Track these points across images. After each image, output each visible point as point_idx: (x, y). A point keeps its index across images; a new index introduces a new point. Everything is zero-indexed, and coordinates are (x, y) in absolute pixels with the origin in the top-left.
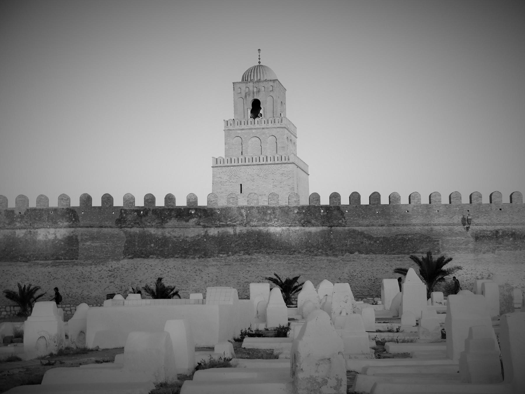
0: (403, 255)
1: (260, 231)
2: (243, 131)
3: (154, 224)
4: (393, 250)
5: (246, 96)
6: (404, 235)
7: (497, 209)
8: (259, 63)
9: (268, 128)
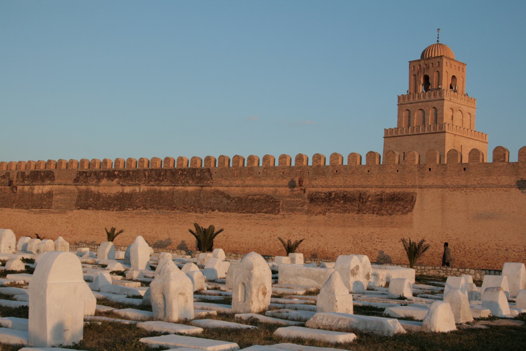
0: (251, 214)
1: (156, 189)
2: (412, 105)
3: (94, 183)
4: (244, 209)
5: (418, 74)
6: (254, 195)
7: (333, 171)
8: (438, 41)
9: (430, 101)
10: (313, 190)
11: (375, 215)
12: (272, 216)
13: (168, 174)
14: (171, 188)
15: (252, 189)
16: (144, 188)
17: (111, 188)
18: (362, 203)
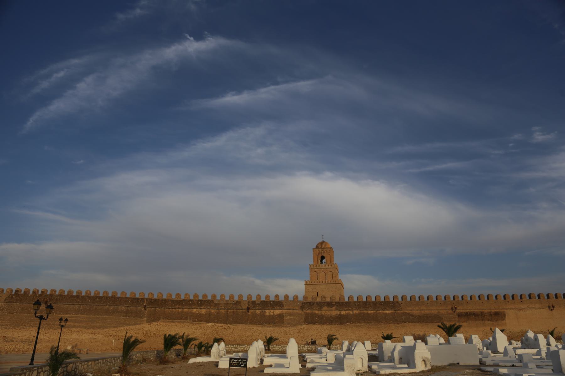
13: (371, 304)
15: (426, 311)
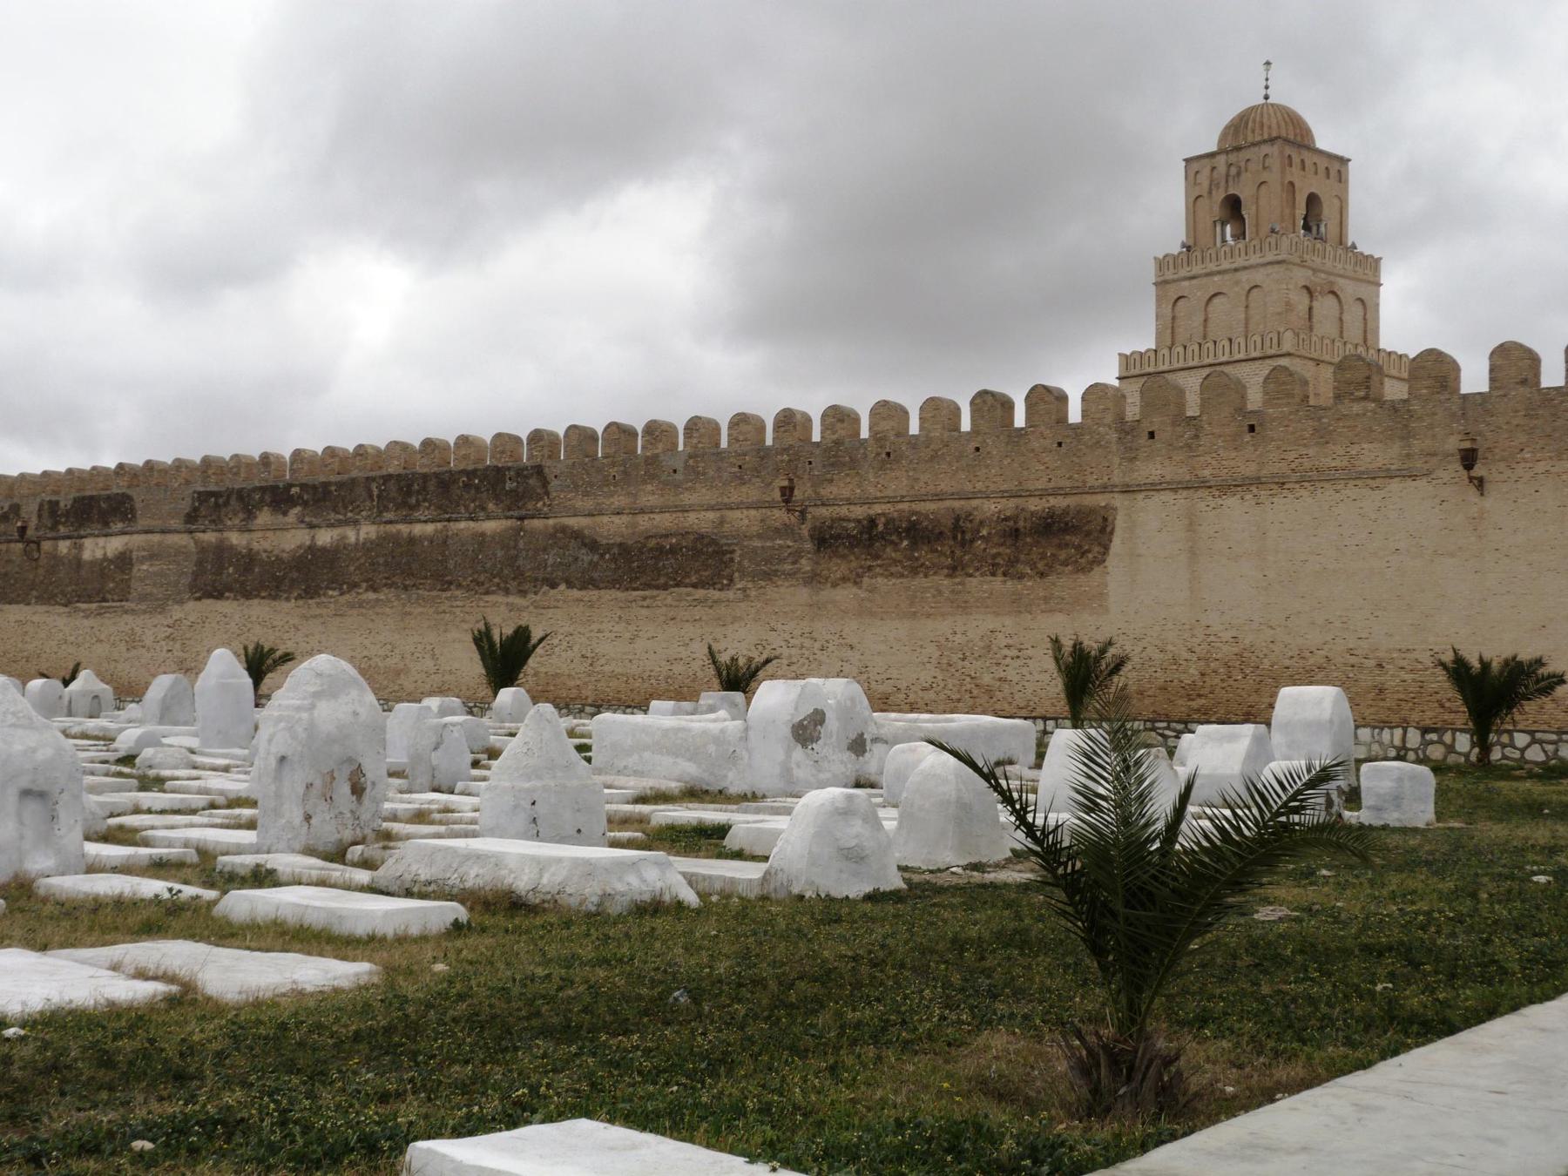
0: (655, 592)
1: (399, 532)
2: (1194, 282)
7: (878, 454)
8: (1266, 97)
10: (824, 512)
11: (1001, 579)
12: (715, 594)
13: (432, 485)
14: (439, 525)
15: (658, 517)
16: (368, 531)
17: (284, 536)
18: (963, 544)
